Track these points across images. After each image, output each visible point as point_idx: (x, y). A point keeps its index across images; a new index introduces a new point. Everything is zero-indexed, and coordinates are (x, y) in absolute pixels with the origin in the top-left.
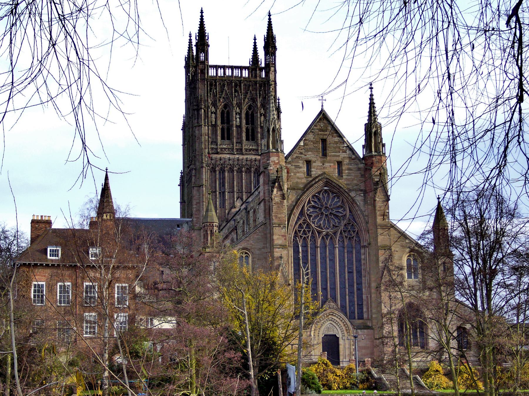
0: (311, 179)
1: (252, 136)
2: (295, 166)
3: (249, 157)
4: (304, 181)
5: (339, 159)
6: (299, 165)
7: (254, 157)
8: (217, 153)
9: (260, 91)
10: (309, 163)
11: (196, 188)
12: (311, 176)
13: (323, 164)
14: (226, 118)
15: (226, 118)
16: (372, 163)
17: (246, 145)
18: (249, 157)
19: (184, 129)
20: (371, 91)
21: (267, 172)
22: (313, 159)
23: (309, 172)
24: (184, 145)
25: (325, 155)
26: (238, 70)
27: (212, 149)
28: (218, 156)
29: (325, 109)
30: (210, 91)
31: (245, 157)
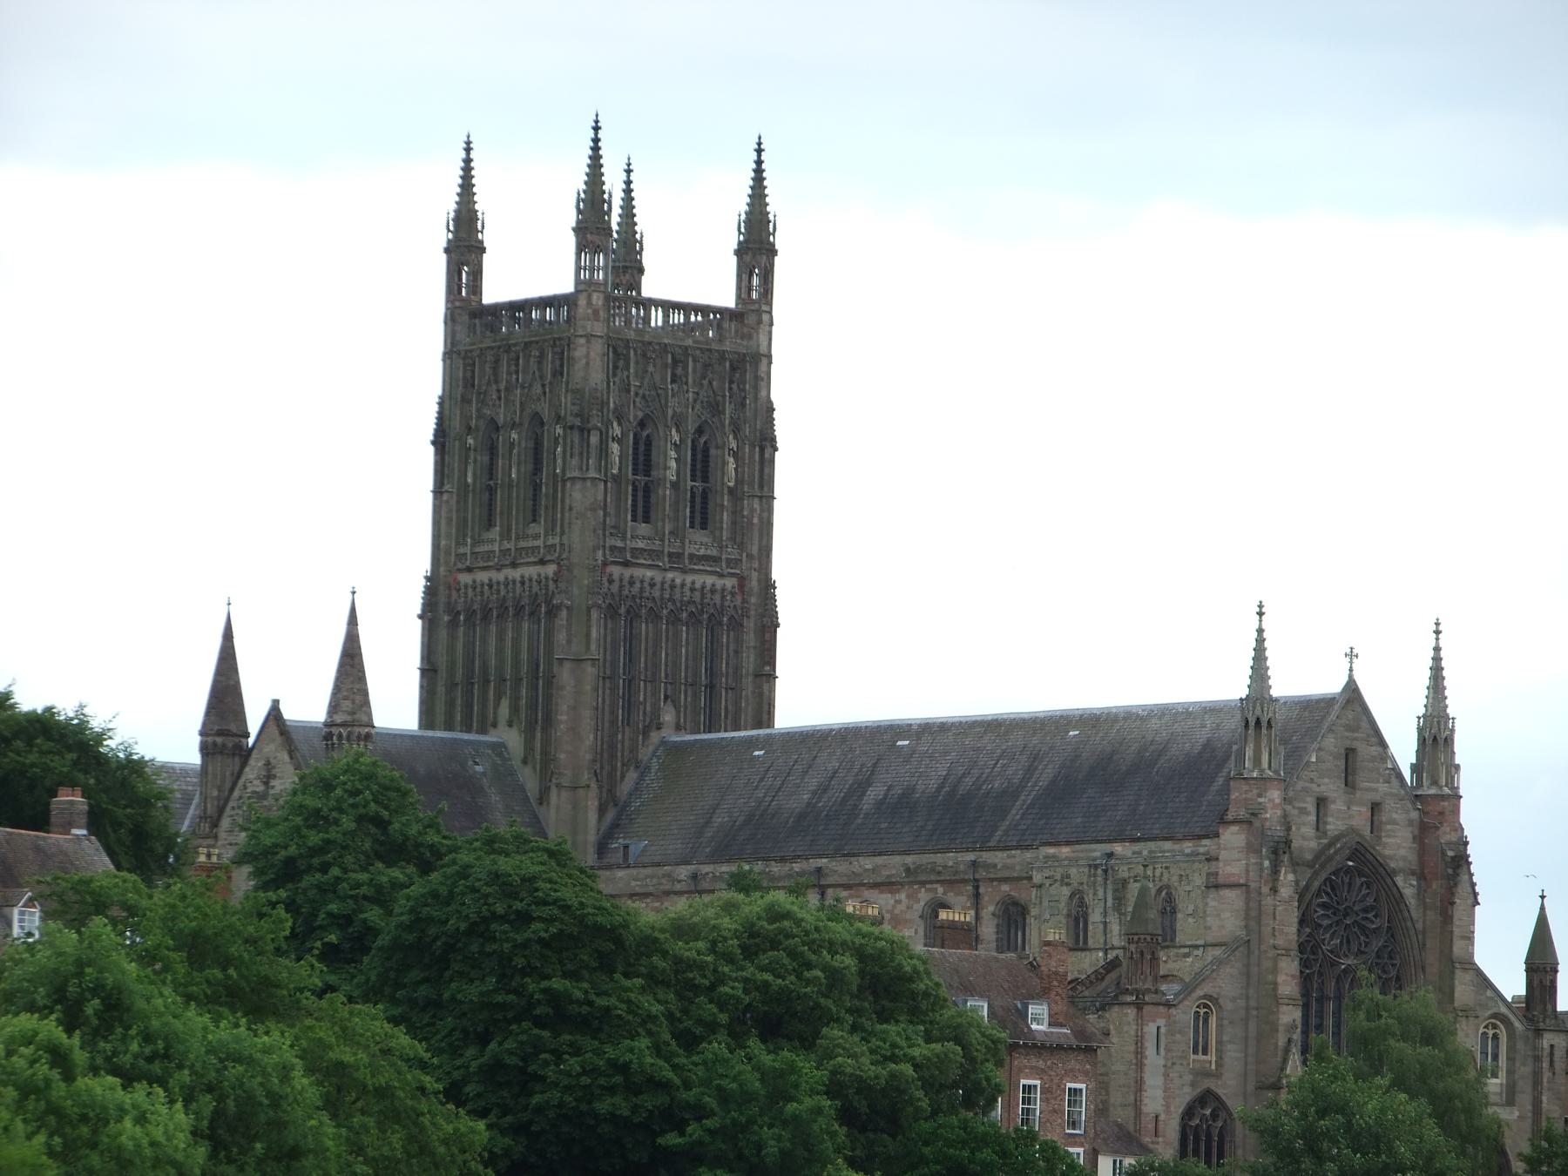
0: (1325, 841)
1: (702, 517)
2: (1300, 808)
3: (699, 580)
4: (1313, 844)
5: (1377, 798)
6: (1305, 808)
7: (710, 580)
8: (626, 564)
9: (731, 382)
10: (1321, 802)
11: (567, 666)
12: (1325, 833)
13: (1349, 808)
14: (643, 459)
15: (643, 459)
16: (1441, 813)
17: (699, 543)
18: (699, 580)
19: (441, 440)
20: (1437, 639)
21: (1257, 823)
22: (1332, 795)
23: (1319, 826)
24: (438, 491)
25: (1349, 782)
26: (679, 314)
27: (613, 548)
28: (628, 572)
29: (1356, 677)
30: (615, 375)
31: (689, 579)
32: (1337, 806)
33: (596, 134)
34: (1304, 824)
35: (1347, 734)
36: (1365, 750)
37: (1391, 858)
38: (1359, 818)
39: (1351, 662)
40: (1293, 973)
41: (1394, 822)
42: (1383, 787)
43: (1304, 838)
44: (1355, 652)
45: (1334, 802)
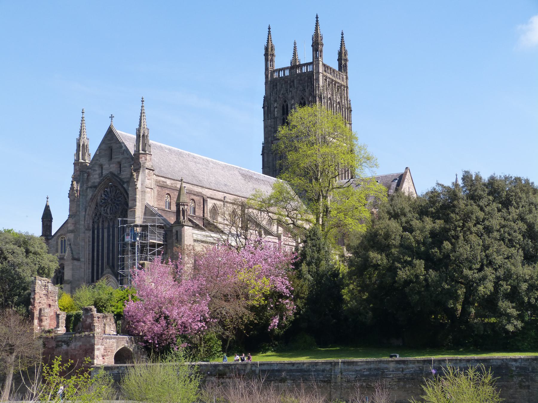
2: (93, 170)
6: (95, 169)
13: (110, 166)
32: (106, 166)
33: (317, 19)
34: (95, 174)
35: (109, 142)
36: (114, 146)
37: (124, 178)
38: (114, 168)
39: (112, 119)
40: (73, 223)
41: (125, 167)
42: (121, 157)
43: (95, 179)
44: (113, 116)
45: (104, 165)
